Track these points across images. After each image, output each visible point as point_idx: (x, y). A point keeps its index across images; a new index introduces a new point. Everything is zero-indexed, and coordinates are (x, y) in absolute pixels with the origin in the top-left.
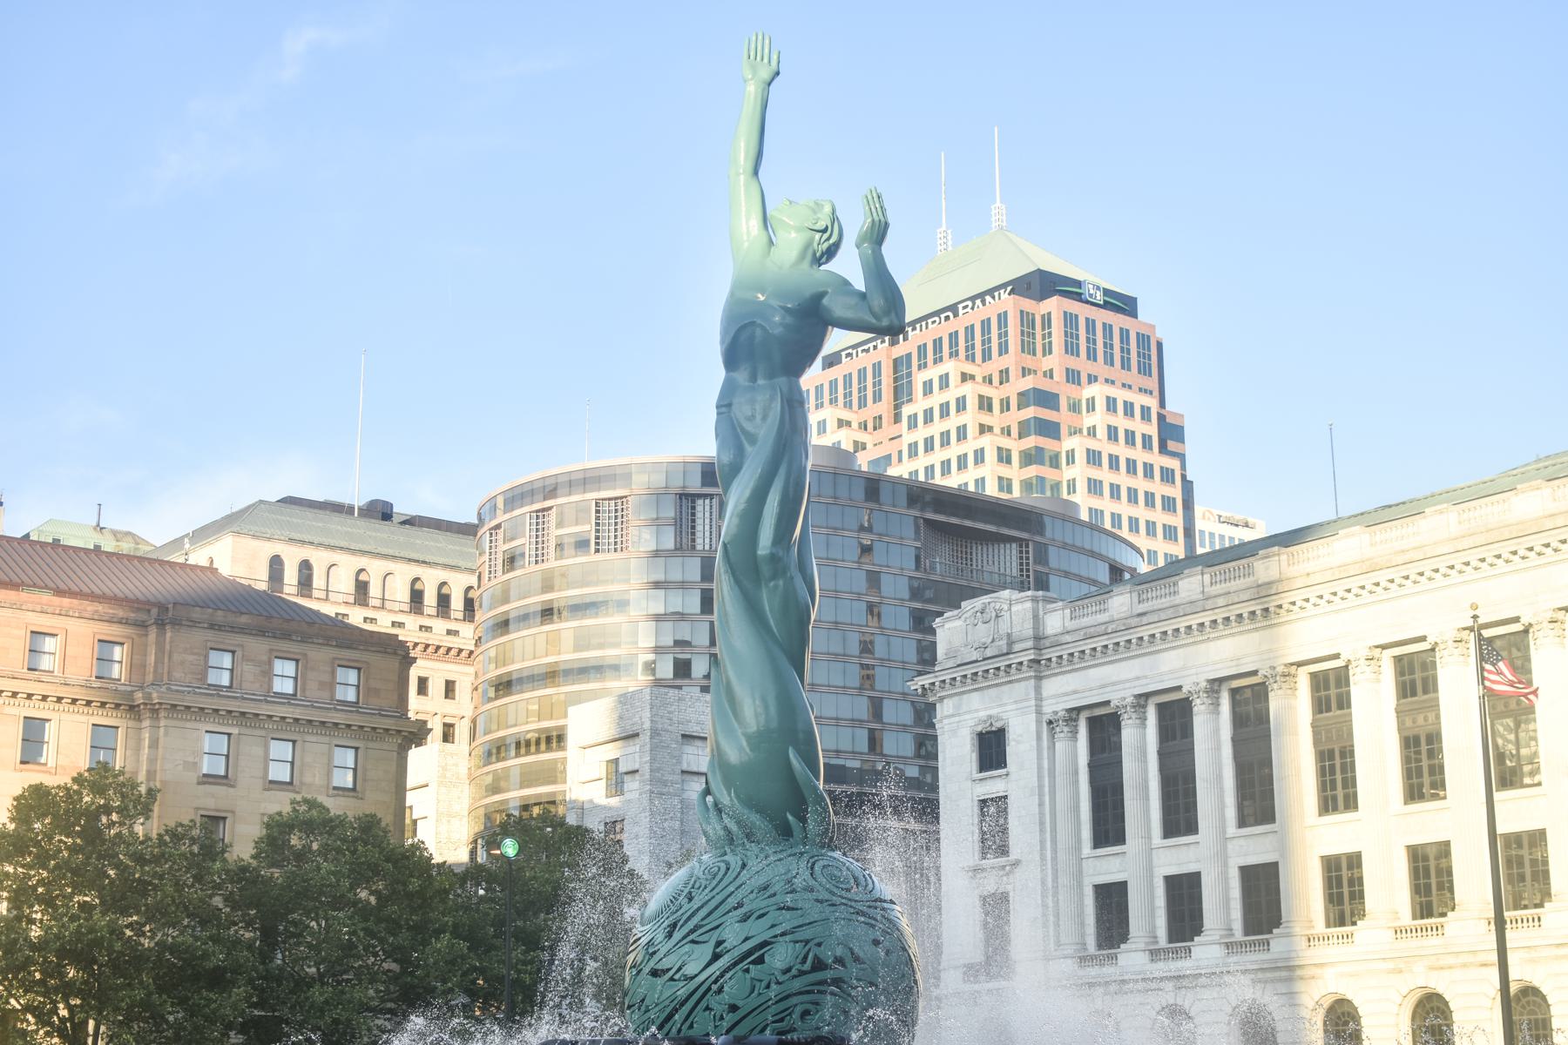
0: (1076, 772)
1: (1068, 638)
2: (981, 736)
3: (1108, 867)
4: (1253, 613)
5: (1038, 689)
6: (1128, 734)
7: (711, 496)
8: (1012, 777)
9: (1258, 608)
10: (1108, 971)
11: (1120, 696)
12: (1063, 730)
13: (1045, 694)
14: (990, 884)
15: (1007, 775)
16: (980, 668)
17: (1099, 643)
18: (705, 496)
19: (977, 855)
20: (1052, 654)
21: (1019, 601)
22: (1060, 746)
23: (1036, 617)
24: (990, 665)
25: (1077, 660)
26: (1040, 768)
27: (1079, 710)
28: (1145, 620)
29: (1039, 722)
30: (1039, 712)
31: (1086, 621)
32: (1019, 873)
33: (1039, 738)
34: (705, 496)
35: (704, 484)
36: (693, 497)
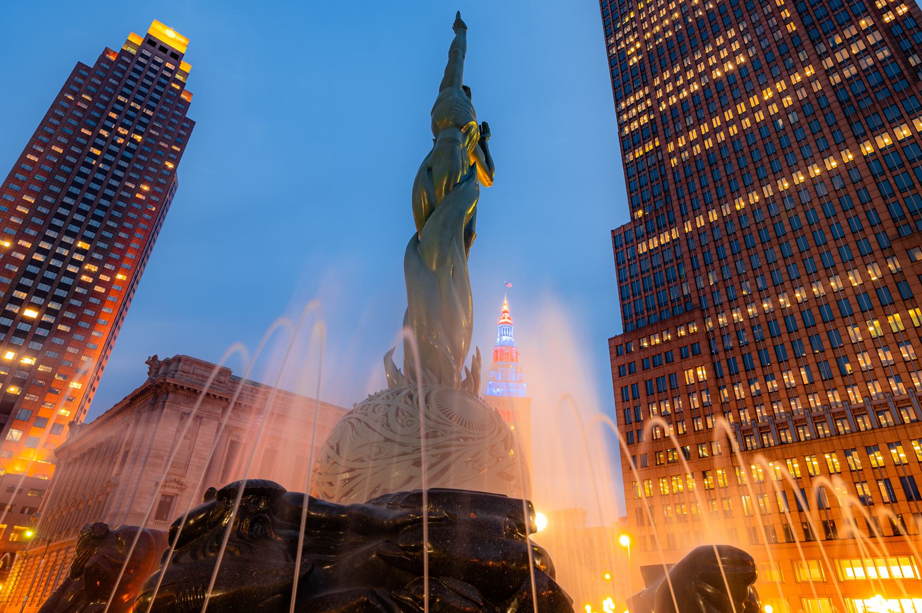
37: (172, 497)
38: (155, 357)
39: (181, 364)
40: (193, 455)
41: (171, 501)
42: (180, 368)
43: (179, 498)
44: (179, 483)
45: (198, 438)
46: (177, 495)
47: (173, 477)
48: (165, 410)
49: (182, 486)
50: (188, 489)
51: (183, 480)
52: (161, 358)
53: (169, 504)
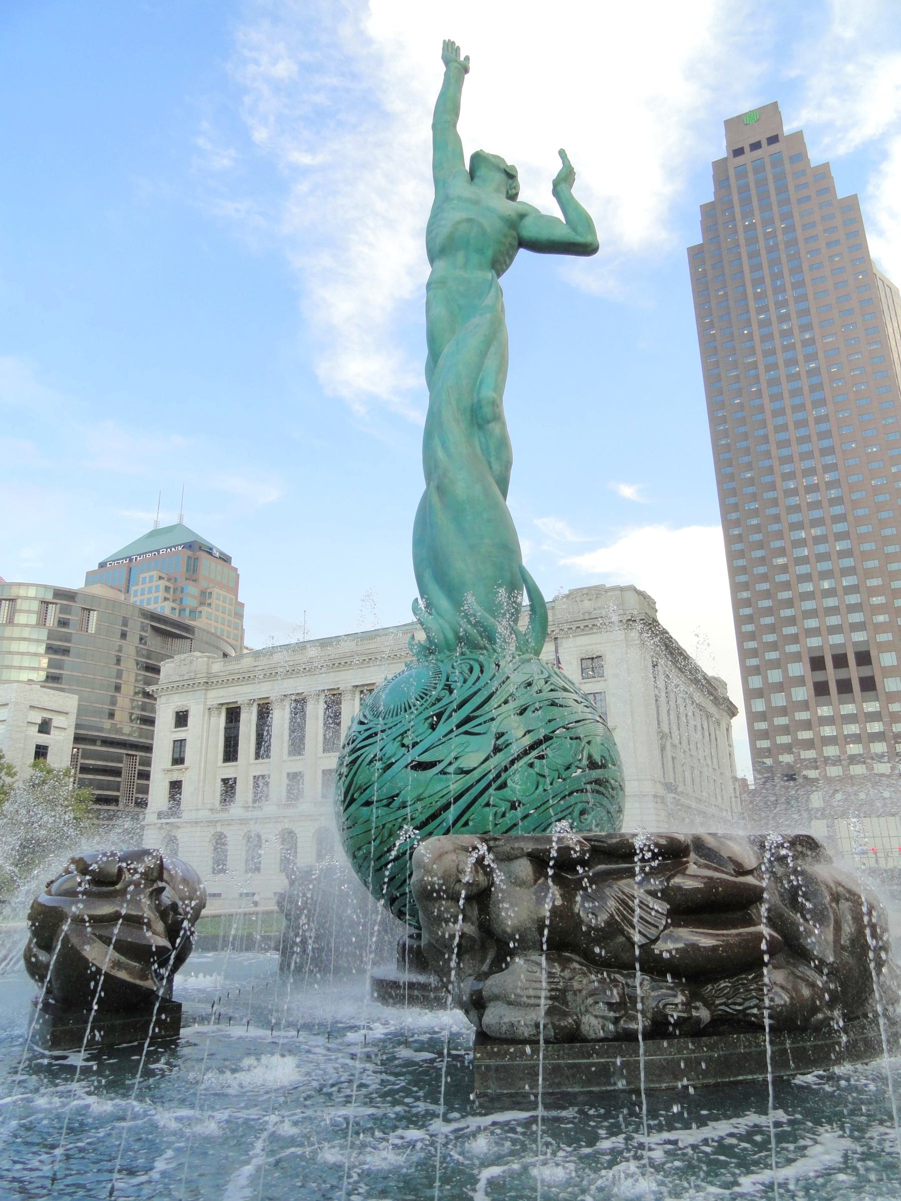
0: (218, 731)
1: (221, 674)
2: (177, 713)
3: (229, 771)
5: (206, 695)
6: (243, 716)
7: (56, 604)
10: (223, 816)
11: (241, 700)
12: (215, 713)
13: (208, 696)
14: (175, 777)
16: (180, 684)
18: (53, 603)
21: (201, 657)
23: (208, 664)
24: (186, 683)
25: (226, 683)
26: (203, 728)
27: (222, 704)
28: (256, 669)
30: (205, 704)
31: (230, 668)
32: (188, 773)
33: (204, 715)
34: (53, 603)
35: (54, 597)
36: (47, 603)
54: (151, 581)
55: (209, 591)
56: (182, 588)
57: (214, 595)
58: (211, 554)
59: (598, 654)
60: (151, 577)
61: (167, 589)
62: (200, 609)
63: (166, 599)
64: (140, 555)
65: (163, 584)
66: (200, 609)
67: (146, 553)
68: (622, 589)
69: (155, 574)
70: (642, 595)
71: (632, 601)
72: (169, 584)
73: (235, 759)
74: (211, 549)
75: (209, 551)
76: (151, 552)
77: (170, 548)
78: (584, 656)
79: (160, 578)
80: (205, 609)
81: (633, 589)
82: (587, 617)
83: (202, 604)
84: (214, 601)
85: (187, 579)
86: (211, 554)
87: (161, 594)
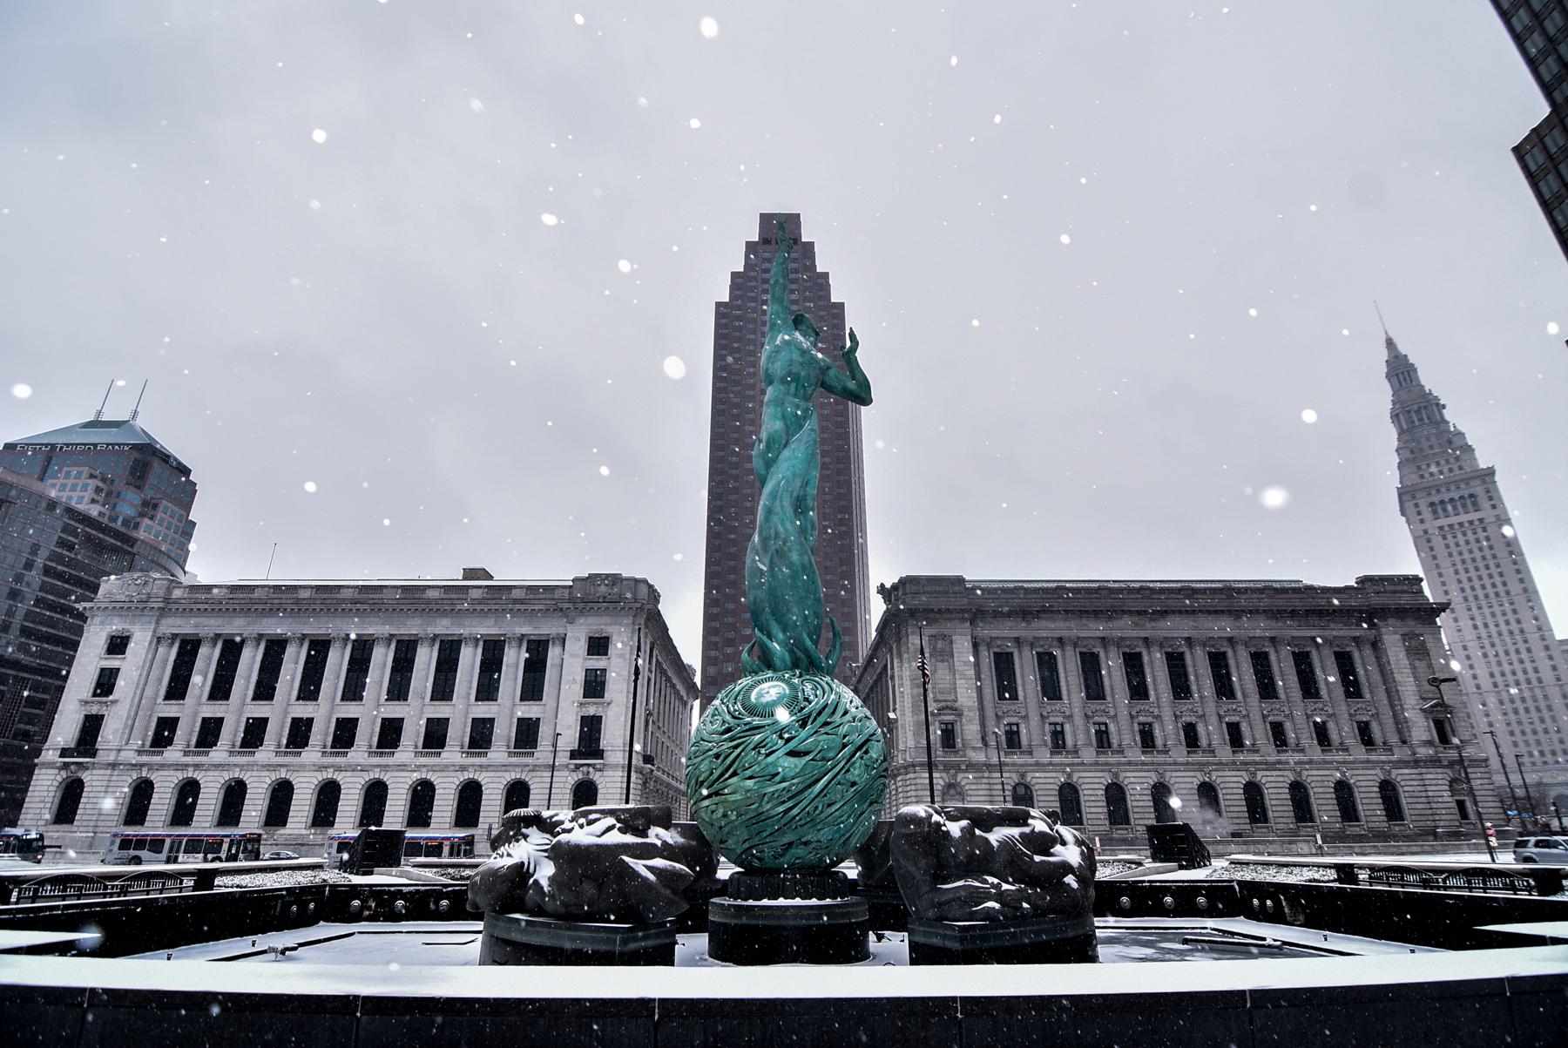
4: (292, 609)
8: (127, 660)
9: (296, 608)
15: (124, 658)
17: (202, 607)
19: (90, 695)
20: (174, 607)
22: (161, 650)
29: (153, 636)
37: (952, 724)
38: (882, 585)
39: (908, 585)
40: (957, 677)
41: (953, 727)
42: (908, 591)
43: (959, 724)
44: (951, 709)
45: (955, 659)
46: (956, 721)
47: (943, 704)
48: (910, 637)
49: (959, 713)
50: (965, 713)
51: (957, 705)
52: (888, 586)
53: (953, 730)
54: (78, 476)
55: (154, 501)
56: (119, 493)
57: (161, 508)
58: (167, 462)
59: (604, 635)
60: (79, 473)
61: (98, 490)
62: (138, 520)
63: (93, 501)
64: (68, 445)
65: (93, 483)
66: (138, 520)
67: (78, 444)
68: (637, 581)
69: (86, 470)
70: (651, 587)
71: (643, 590)
72: (101, 485)
73: (182, 696)
74: (168, 456)
75: (166, 458)
76: (85, 445)
77: (113, 445)
78: (592, 635)
79: (92, 476)
80: (146, 521)
81: (645, 581)
82: (600, 600)
83: (142, 515)
84: (159, 515)
85: (127, 484)
86: (167, 462)
87: (89, 494)
